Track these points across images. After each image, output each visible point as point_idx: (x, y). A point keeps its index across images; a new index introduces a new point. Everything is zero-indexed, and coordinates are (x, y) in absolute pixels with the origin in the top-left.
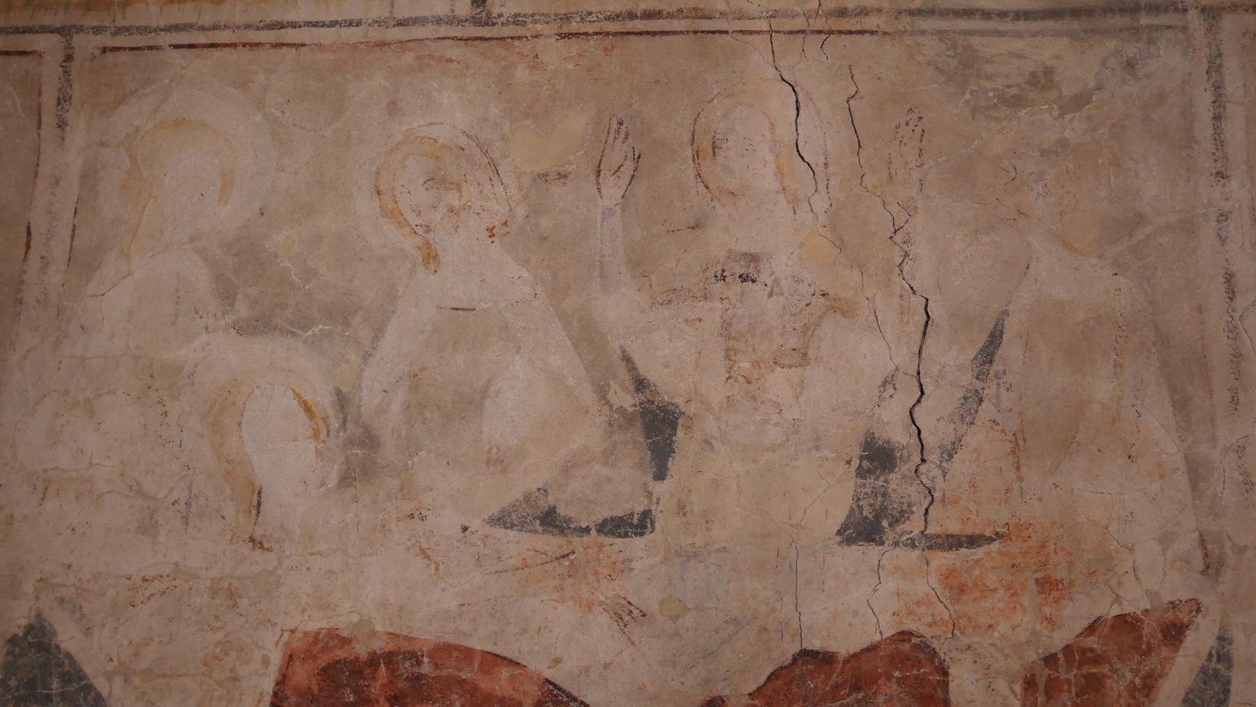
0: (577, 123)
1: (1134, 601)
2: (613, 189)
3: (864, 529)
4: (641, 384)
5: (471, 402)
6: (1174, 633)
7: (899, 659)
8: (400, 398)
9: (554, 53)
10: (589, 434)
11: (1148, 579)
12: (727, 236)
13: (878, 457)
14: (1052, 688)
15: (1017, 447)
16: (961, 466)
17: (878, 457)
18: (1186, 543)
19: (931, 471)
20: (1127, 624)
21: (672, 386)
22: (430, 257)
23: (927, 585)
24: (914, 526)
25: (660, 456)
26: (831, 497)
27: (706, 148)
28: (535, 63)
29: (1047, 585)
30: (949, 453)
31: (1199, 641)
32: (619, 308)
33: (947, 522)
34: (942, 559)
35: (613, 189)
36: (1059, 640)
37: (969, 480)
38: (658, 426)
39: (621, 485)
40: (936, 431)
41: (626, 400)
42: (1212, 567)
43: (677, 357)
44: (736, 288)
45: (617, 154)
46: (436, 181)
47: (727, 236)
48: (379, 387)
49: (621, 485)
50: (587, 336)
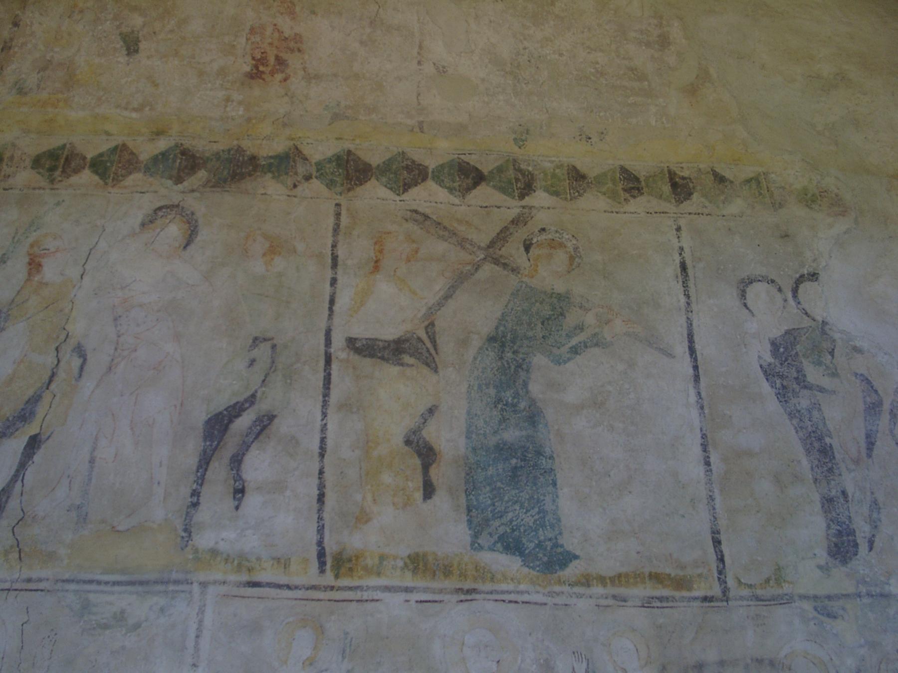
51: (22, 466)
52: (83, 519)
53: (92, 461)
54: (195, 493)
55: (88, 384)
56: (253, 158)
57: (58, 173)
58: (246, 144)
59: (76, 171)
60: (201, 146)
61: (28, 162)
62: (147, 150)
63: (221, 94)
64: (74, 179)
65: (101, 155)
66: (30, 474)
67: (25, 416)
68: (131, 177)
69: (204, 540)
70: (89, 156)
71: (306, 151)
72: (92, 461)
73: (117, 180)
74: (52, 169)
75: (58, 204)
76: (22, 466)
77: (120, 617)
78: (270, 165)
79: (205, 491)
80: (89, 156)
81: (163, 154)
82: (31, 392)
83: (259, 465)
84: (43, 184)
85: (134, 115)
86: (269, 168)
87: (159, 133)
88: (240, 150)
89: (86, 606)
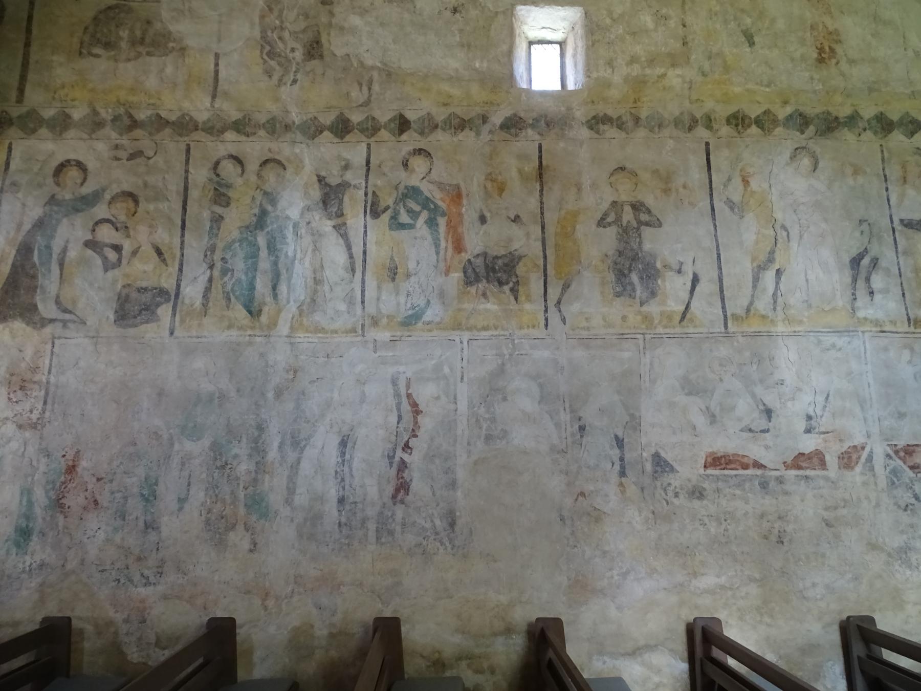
0: (747, 354)
1: (856, 443)
2: (755, 367)
3: (808, 431)
4: (764, 405)
5: (733, 408)
6: (863, 448)
7: (816, 454)
8: (718, 409)
9: (741, 339)
10: (756, 414)
11: (859, 440)
12: (777, 376)
13: (809, 418)
14: (843, 458)
15: (833, 415)
16: (824, 419)
17: (809, 418)
18: (864, 432)
19: (818, 420)
20: (855, 447)
21: (770, 405)
22: (721, 380)
23: (820, 441)
24: (817, 430)
25: (769, 418)
26: (801, 425)
27: (772, 359)
28: (738, 342)
29: (841, 440)
30: (822, 417)
31: (867, 449)
32: (759, 390)
33: (823, 429)
34: (822, 436)
35: (755, 367)
36: (843, 450)
37: (825, 423)
38: (769, 413)
39: (763, 424)
40: (819, 413)
41: (762, 407)
42: (869, 437)
43: (770, 399)
44: (780, 386)
45: (755, 360)
46: (721, 365)
47: (777, 376)
48: (714, 406)
49: (763, 424)
50: (754, 396)
51: (777, 283)
52: (810, 306)
53: (807, 280)
54: (853, 294)
55: (794, 244)
56: (837, 118)
57: (740, 127)
58: (831, 109)
59: (749, 126)
60: (809, 111)
61: (724, 122)
62: (782, 113)
63: (807, 74)
64: (749, 131)
65: (758, 116)
66: (782, 286)
67: (771, 260)
68: (777, 129)
69: (861, 314)
70: (753, 117)
71: (861, 113)
72: (807, 280)
73: (770, 131)
74: (737, 125)
75: (747, 146)
76: (777, 283)
77: (834, 346)
78: (846, 122)
79: (857, 293)
80: (753, 117)
81: (790, 115)
82: (768, 249)
83: (877, 281)
84: (736, 134)
85: (767, 90)
86: (845, 124)
87: (786, 103)
88: (829, 113)
89: (820, 342)
